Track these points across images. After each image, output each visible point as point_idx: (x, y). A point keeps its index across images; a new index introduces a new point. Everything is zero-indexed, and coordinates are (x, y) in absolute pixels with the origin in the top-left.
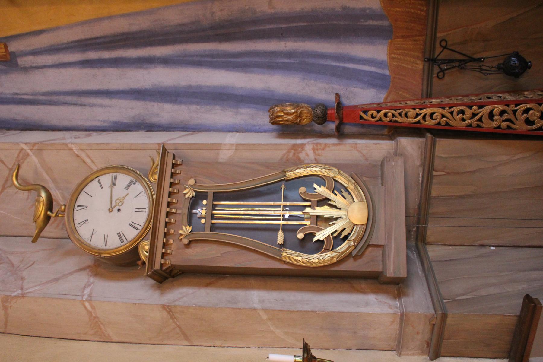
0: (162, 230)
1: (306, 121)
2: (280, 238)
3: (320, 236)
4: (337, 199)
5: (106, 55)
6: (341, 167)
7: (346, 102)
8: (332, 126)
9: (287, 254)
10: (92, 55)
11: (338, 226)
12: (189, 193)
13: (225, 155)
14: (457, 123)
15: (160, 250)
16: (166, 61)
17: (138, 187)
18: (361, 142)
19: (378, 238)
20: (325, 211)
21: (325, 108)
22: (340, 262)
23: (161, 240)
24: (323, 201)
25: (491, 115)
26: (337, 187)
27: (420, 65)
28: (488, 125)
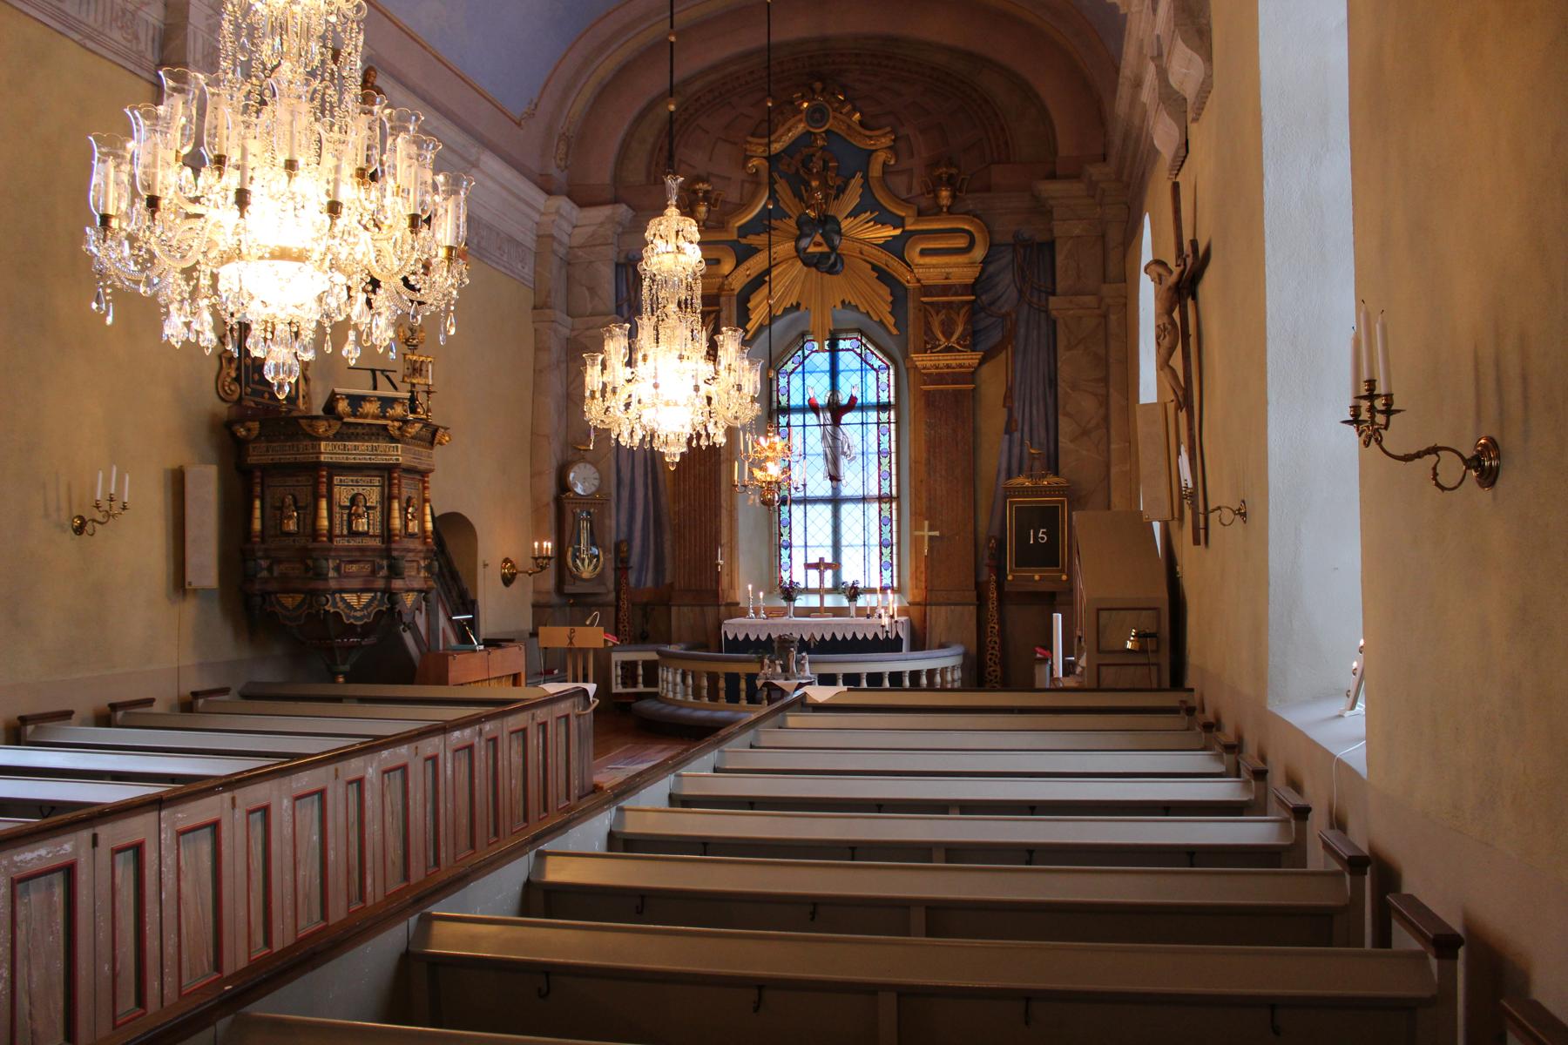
0: (578, 501)
1: (622, 555)
2: (577, 546)
3: (578, 561)
4: (591, 567)
5: (649, 469)
6: (603, 569)
7: (630, 571)
8: (620, 566)
9: (570, 549)
10: (649, 463)
11: (581, 568)
12: (592, 510)
13: (607, 522)
14: (621, 614)
15: (571, 501)
16: (646, 495)
17: (593, 489)
18: (613, 577)
19: (578, 583)
20: (587, 561)
21: (628, 562)
22: (568, 568)
23: (574, 501)
24: (590, 562)
25: (625, 626)
26: (596, 567)
27: (645, 600)
28: (621, 627)
